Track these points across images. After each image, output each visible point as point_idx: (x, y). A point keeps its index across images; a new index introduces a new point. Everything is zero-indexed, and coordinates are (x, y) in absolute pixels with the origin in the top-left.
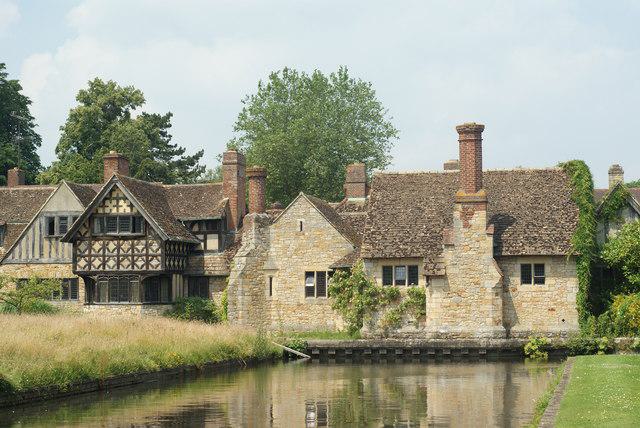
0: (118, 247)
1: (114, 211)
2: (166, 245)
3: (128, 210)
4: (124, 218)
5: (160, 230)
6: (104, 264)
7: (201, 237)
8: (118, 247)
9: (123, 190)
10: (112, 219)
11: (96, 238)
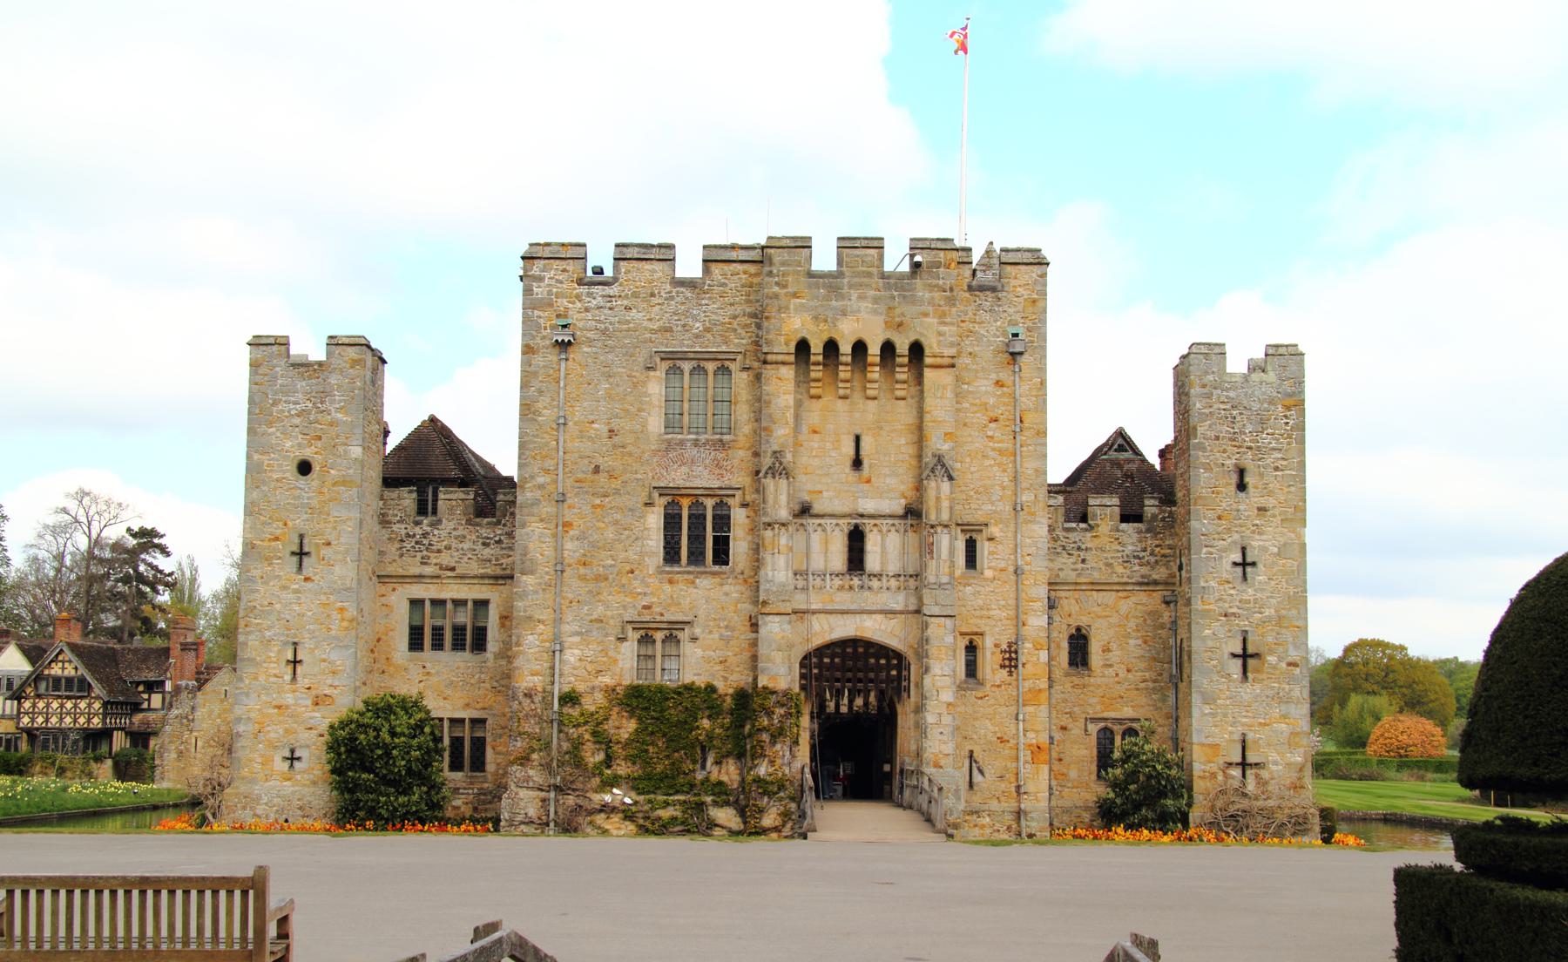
0: (62, 706)
1: (59, 672)
2: (105, 704)
3: (73, 673)
4: (69, 680)
5: (97, 690)
6: (47, 721)
7: (145, 696)
8: (62, 706)
9: (68, 654)
10: (57, 681)
11: (39, 696)
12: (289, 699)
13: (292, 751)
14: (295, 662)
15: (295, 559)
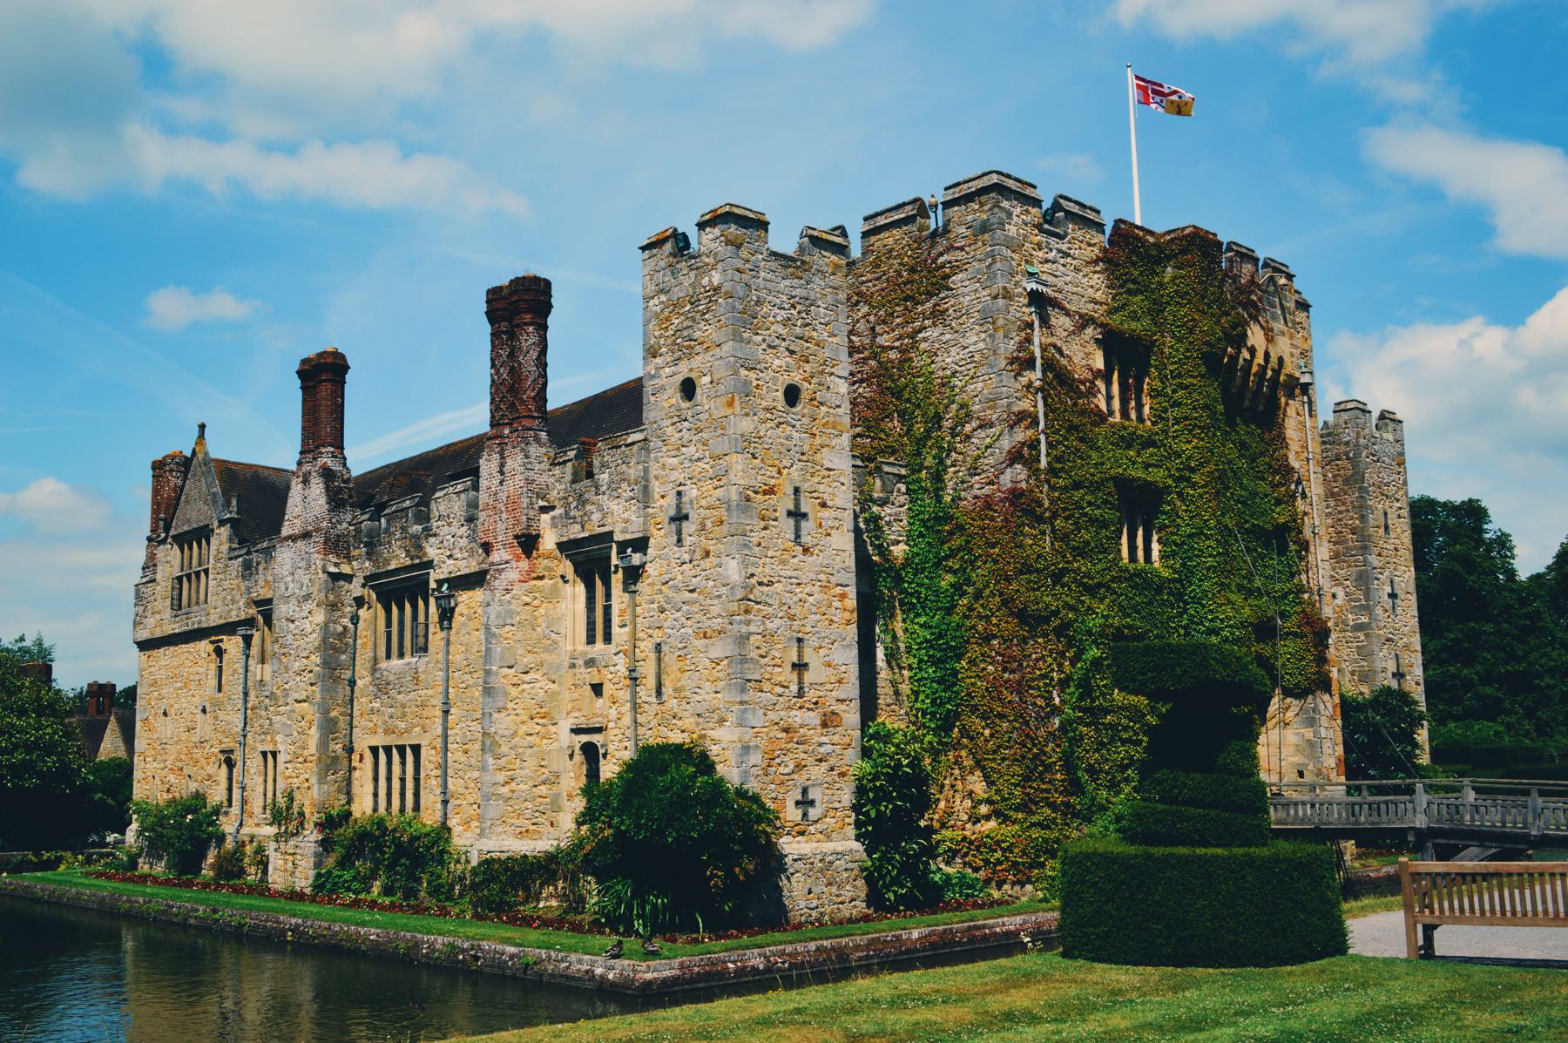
12: (797, 717)
13: (805, 791)
14: (800, 667)
15: (791, 521)
